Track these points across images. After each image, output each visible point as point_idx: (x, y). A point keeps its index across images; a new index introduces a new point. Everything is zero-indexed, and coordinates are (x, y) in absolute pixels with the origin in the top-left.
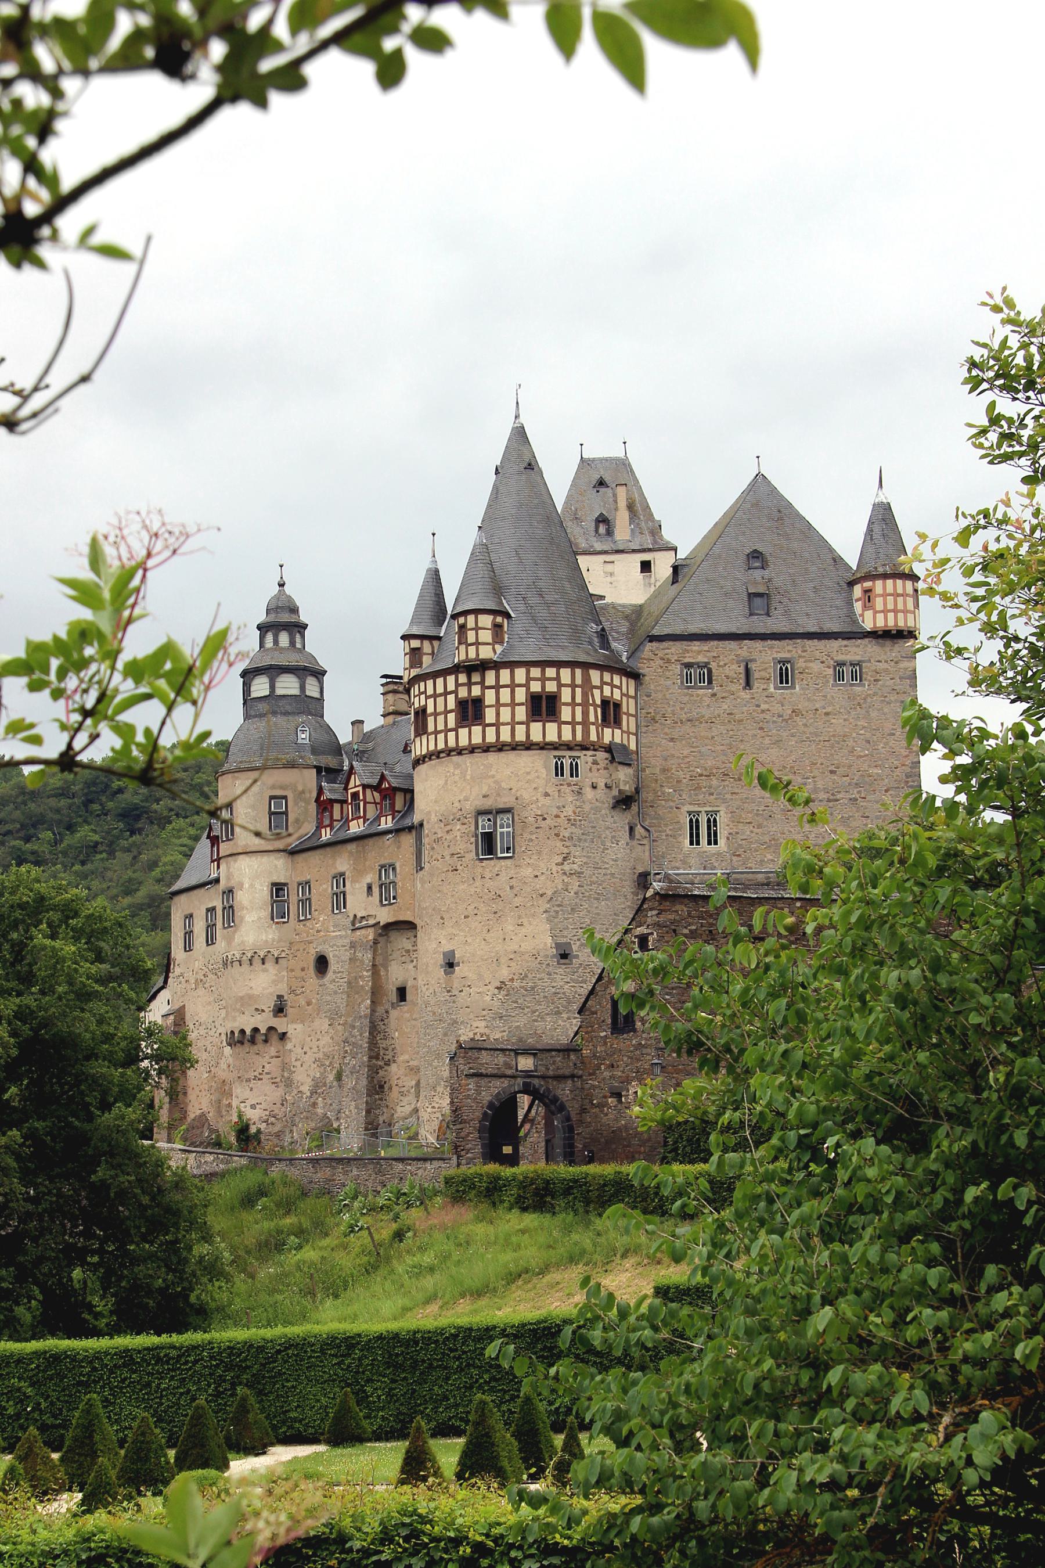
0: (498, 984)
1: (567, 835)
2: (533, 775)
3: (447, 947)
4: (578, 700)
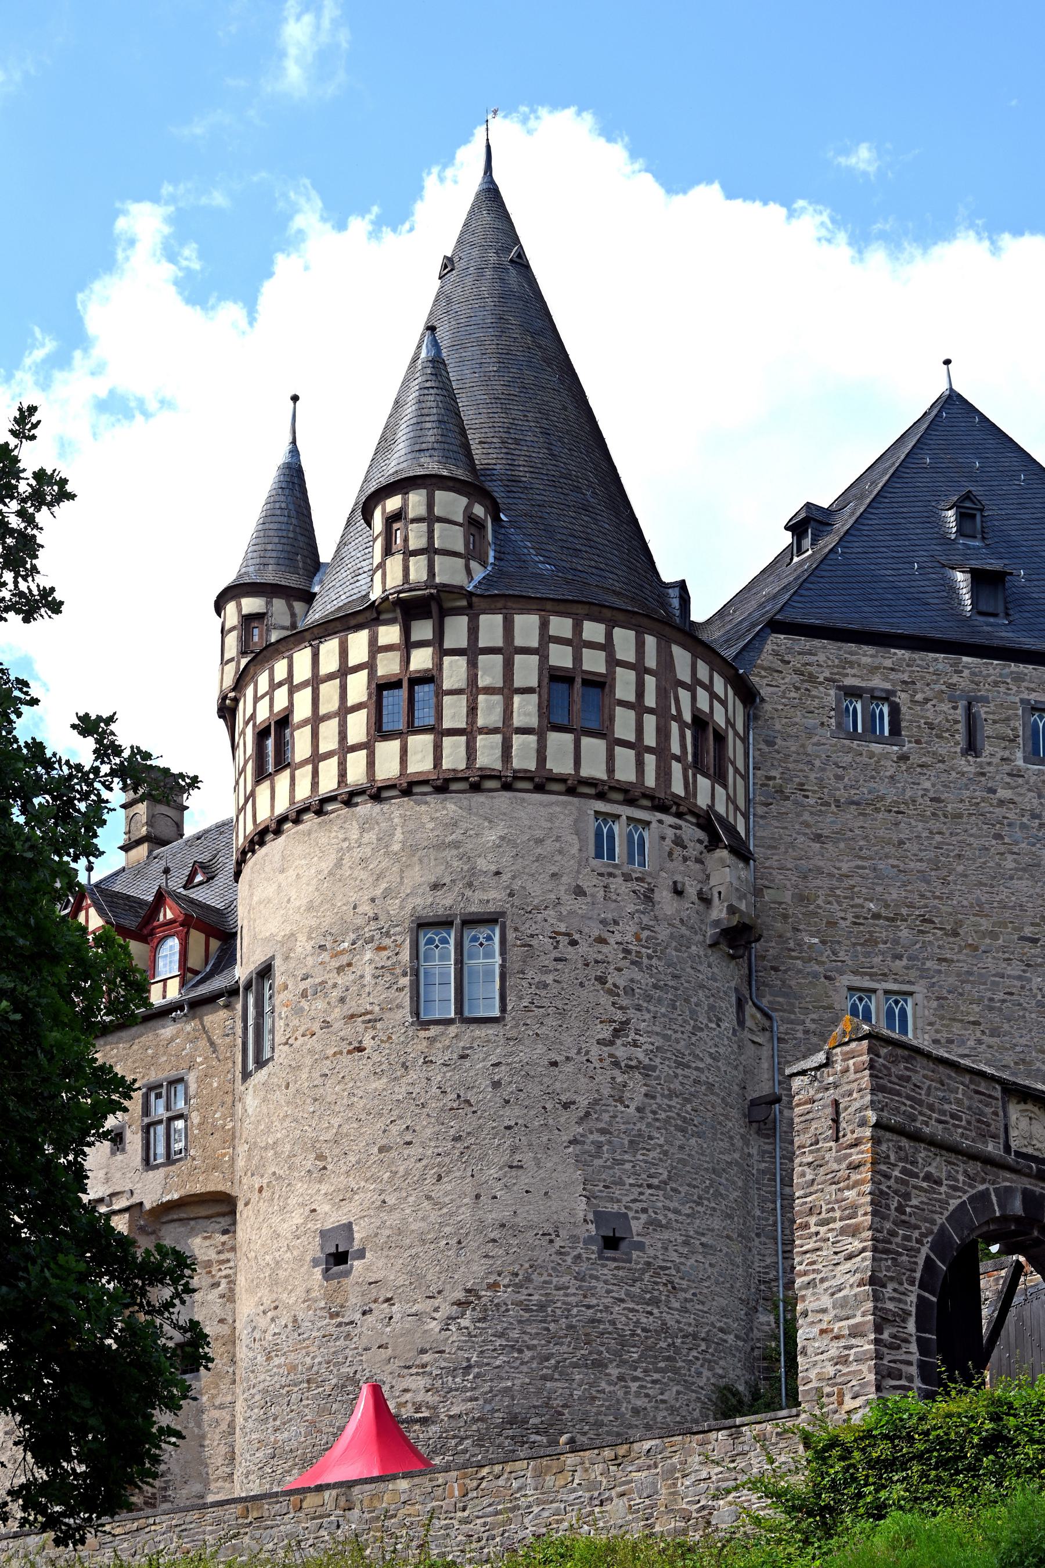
0: (460, 1295)
1: (622, 983)
2: (550, 846)
3: (332, 1217)
4: (650, 701)
